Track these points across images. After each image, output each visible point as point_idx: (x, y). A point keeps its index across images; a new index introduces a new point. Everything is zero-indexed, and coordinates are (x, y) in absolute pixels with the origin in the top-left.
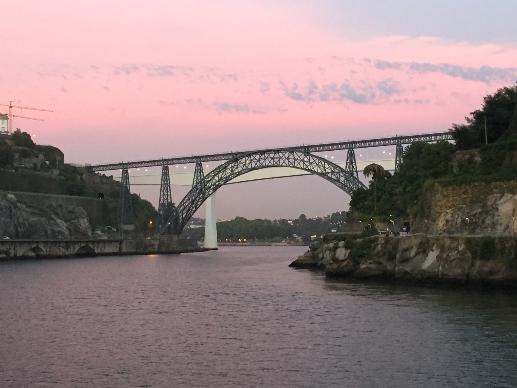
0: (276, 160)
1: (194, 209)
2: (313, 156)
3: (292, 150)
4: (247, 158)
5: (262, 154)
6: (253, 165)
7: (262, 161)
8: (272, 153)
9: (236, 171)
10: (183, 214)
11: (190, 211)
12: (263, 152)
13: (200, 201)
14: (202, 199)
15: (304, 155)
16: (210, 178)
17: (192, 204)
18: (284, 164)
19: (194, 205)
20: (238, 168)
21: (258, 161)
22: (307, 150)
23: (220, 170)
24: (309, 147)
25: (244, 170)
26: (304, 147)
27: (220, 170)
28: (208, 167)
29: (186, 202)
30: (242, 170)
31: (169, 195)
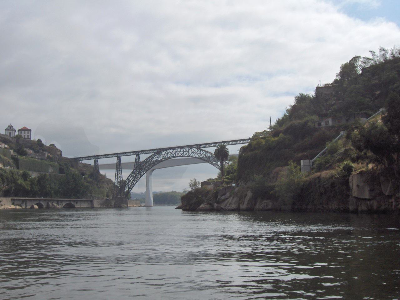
0: (182, 153)
1: (135, 182)
2: (202, 150)
3: (191, 147)
4: (165, 152)
6: (169, 156)
9: (159, 159)
10: (129, 185)
11: (133, 184)
15: (198, 150)
16: (144, 164)
17: (134, 179)
18: (186, 155)
23: (150, 159)
24: (200, 145)
25: (164, 158)
26: (197, 145)
27: (150, 159)
29: (130, 178)
30: (163, 159)
31: (121, 174)
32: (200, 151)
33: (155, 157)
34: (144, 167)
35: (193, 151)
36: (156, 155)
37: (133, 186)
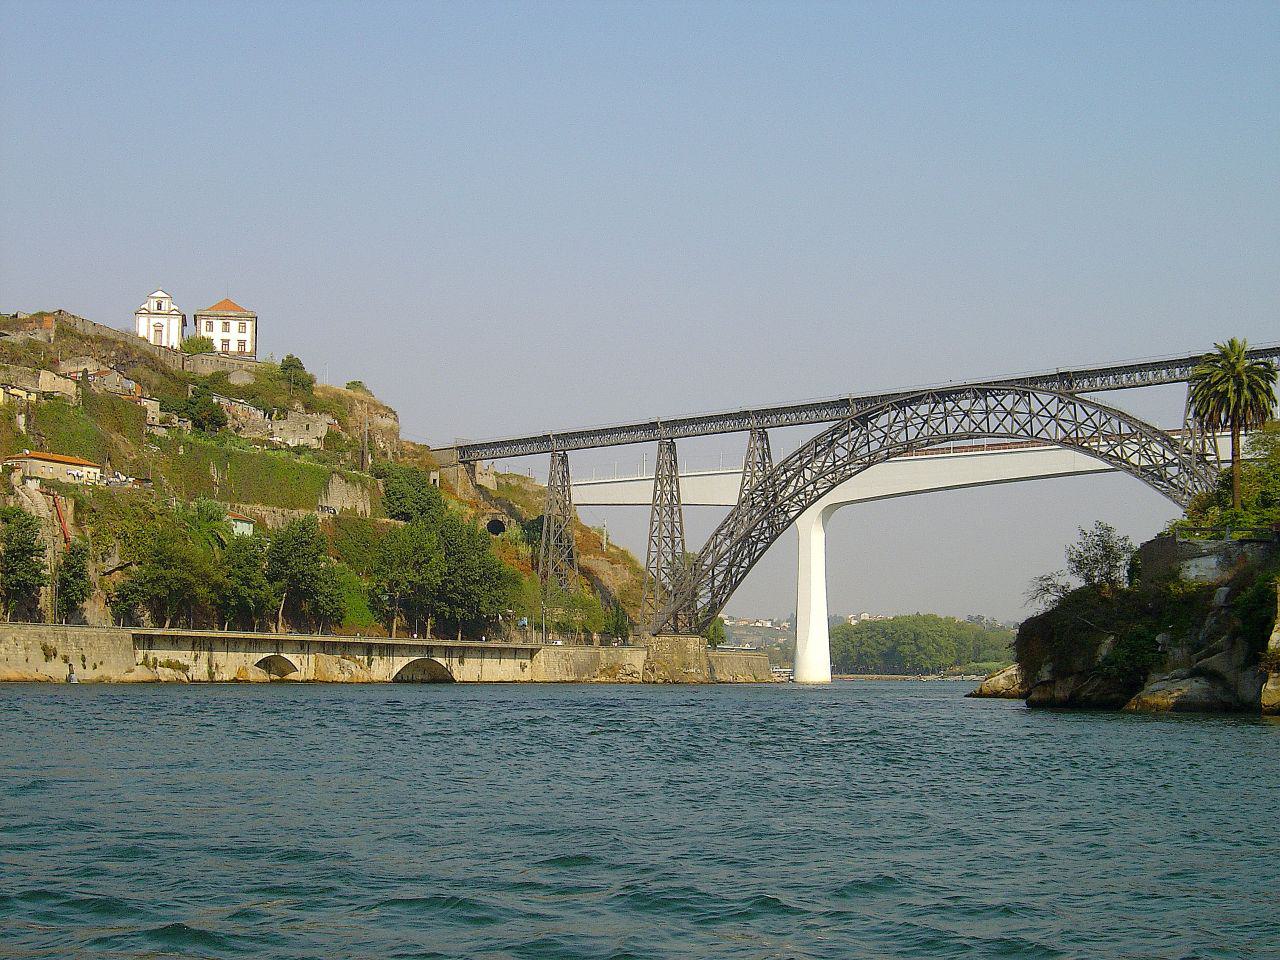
3: (1025, 386)
4: (893, 414)
5: (937, 403)
6: (912, 433)
7: (938, 422)
8: (966, 398)
10: (714, 577)
11: (734, 570)
12: (942, 395)
13: (762, 540)
14: (767, 535)
18: (1001, 430)
19: (746, 552)
20: (868, 442)
21: (926, 422)
22: (1066, 383)
23: (819, 448)
28: (786, 441)
32: (1071, 407)
33: (846, 438)
34: (791, 490)
35: (1036, 407)
36: (847, 433)
37: (737, 583)
